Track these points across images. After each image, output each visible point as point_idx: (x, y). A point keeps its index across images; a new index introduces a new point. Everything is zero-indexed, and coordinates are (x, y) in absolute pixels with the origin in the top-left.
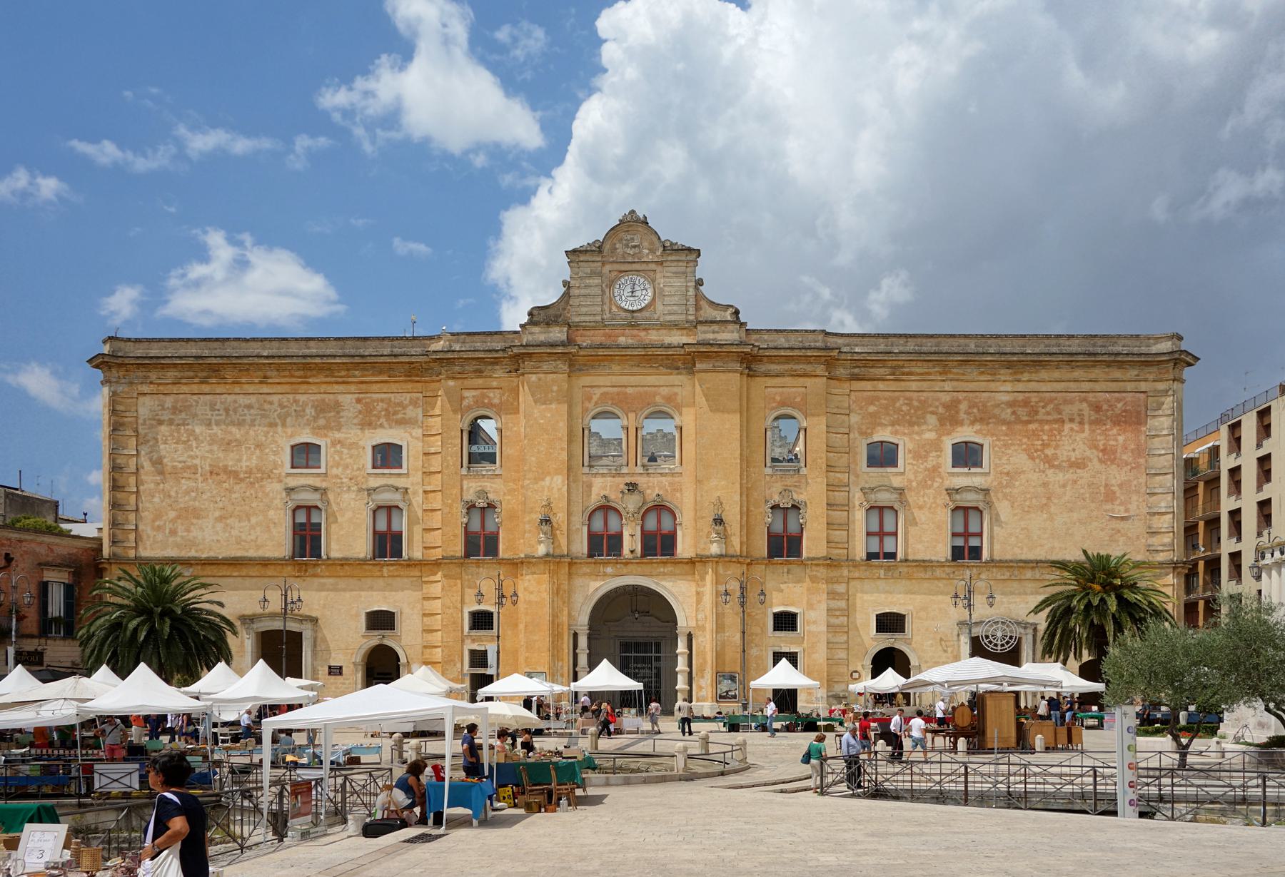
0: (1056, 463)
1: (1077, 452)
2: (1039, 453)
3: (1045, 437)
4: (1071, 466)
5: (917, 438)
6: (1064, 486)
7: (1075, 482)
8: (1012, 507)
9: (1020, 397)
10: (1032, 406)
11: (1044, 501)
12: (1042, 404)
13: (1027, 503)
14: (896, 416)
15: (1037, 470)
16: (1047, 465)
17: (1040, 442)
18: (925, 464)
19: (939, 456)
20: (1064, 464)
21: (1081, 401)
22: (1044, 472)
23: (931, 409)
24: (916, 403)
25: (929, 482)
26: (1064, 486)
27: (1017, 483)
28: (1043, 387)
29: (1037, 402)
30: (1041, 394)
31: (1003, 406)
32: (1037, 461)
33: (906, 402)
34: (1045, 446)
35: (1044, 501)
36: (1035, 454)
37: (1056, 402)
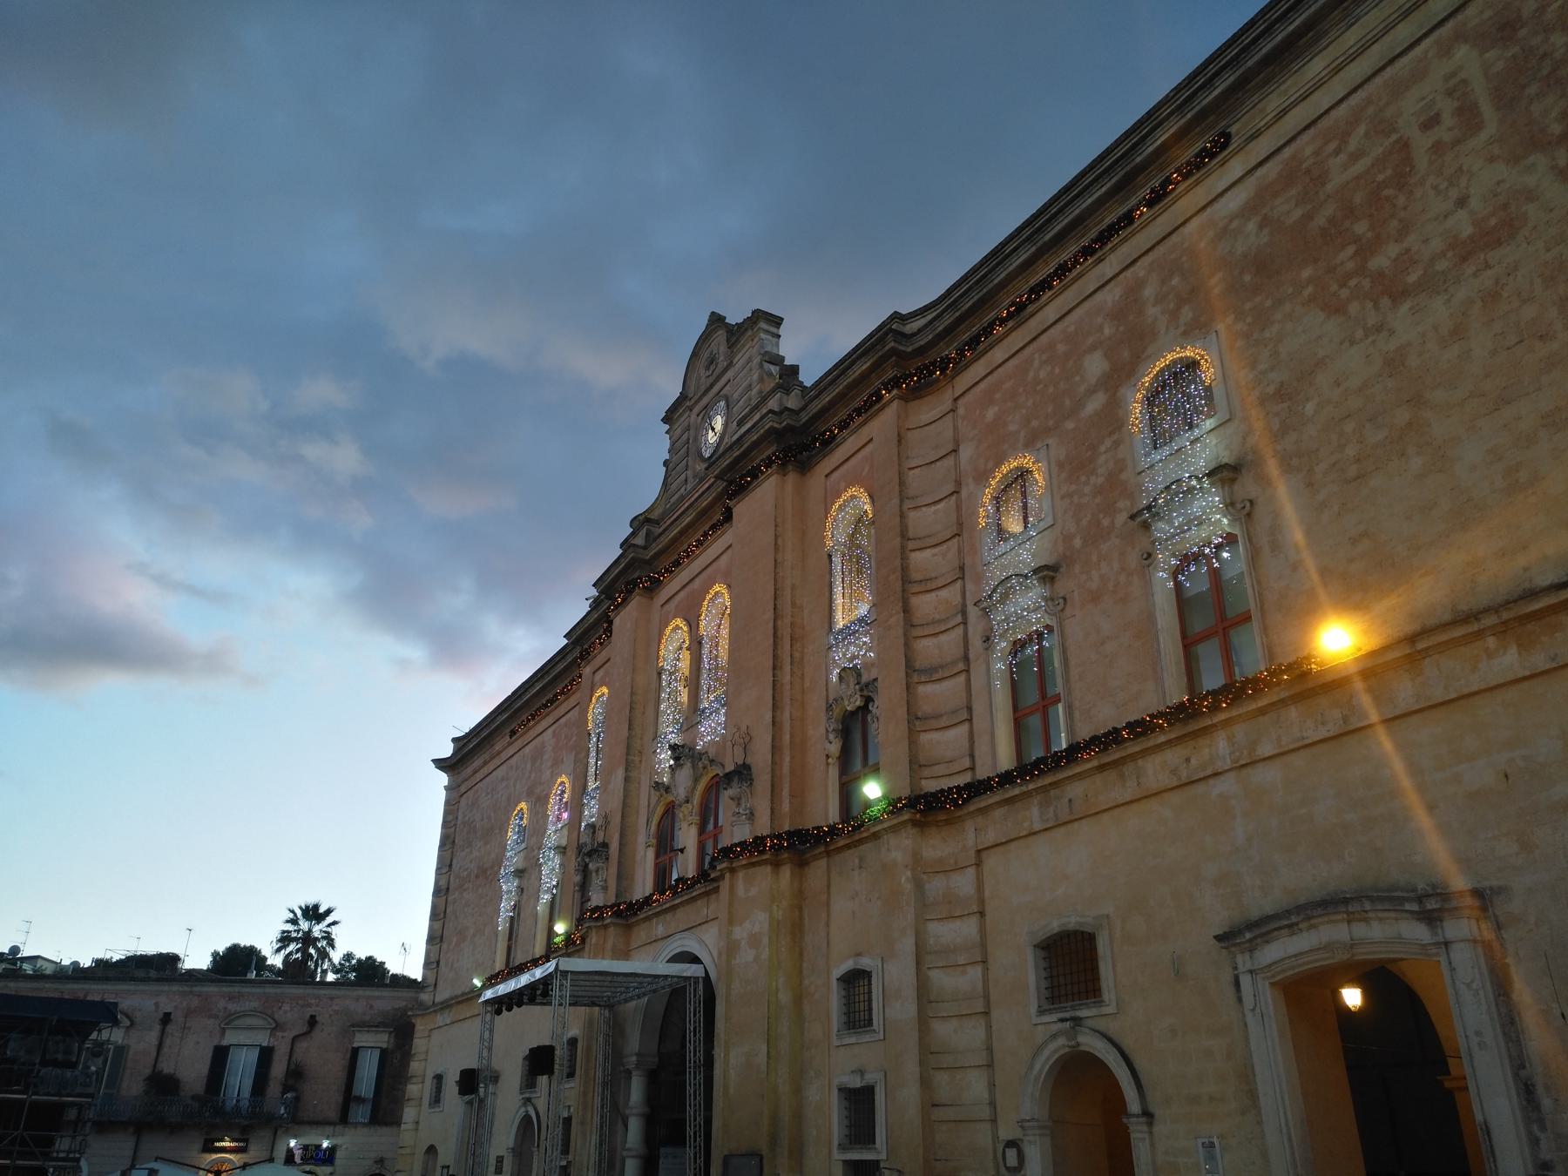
0: (1413, 278)
1: (1475, 203)
2: (1352, 283)
3: (1361, 228)
4: (1464, 259)
5: (1070, 425)
6: (1458, 333)
7: (1492, 297)
8: (1310, 485)
9: (1272, 170)
10: (1308, 171)
11: (1403, 416)
12: (1333, 146)
13: (1351, 451)
14: (1030, 403)
15: (1359, 334)
16: (1385, 302)
17: (1351, 249)
18: (1093, 479)
19: (1117, 444)
20: (1442, 265)
21: (1445, 51)
22: (1379, 328)
23: (1090, 341)
24: (1061, 348)
25: (1106, 522)
26: (1458, 333)
27: (1310, 408)
28: (1323, 99)
29: (1316, 153)
30: (1325, 123)
31: (1235, 224)
32: (1354, 308)
33: (1044, 357)
34: (1366, 250)
35: (1403, 416)
36: (1344, 293)
37: (1371, 110)
